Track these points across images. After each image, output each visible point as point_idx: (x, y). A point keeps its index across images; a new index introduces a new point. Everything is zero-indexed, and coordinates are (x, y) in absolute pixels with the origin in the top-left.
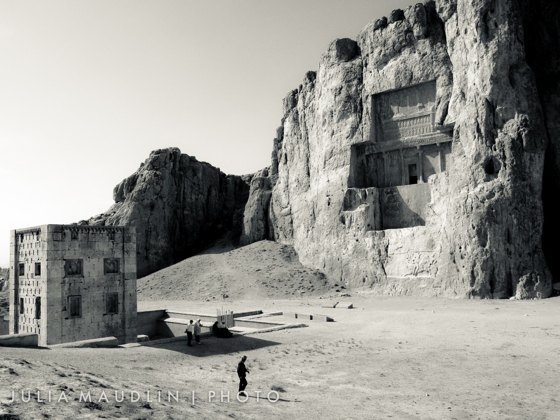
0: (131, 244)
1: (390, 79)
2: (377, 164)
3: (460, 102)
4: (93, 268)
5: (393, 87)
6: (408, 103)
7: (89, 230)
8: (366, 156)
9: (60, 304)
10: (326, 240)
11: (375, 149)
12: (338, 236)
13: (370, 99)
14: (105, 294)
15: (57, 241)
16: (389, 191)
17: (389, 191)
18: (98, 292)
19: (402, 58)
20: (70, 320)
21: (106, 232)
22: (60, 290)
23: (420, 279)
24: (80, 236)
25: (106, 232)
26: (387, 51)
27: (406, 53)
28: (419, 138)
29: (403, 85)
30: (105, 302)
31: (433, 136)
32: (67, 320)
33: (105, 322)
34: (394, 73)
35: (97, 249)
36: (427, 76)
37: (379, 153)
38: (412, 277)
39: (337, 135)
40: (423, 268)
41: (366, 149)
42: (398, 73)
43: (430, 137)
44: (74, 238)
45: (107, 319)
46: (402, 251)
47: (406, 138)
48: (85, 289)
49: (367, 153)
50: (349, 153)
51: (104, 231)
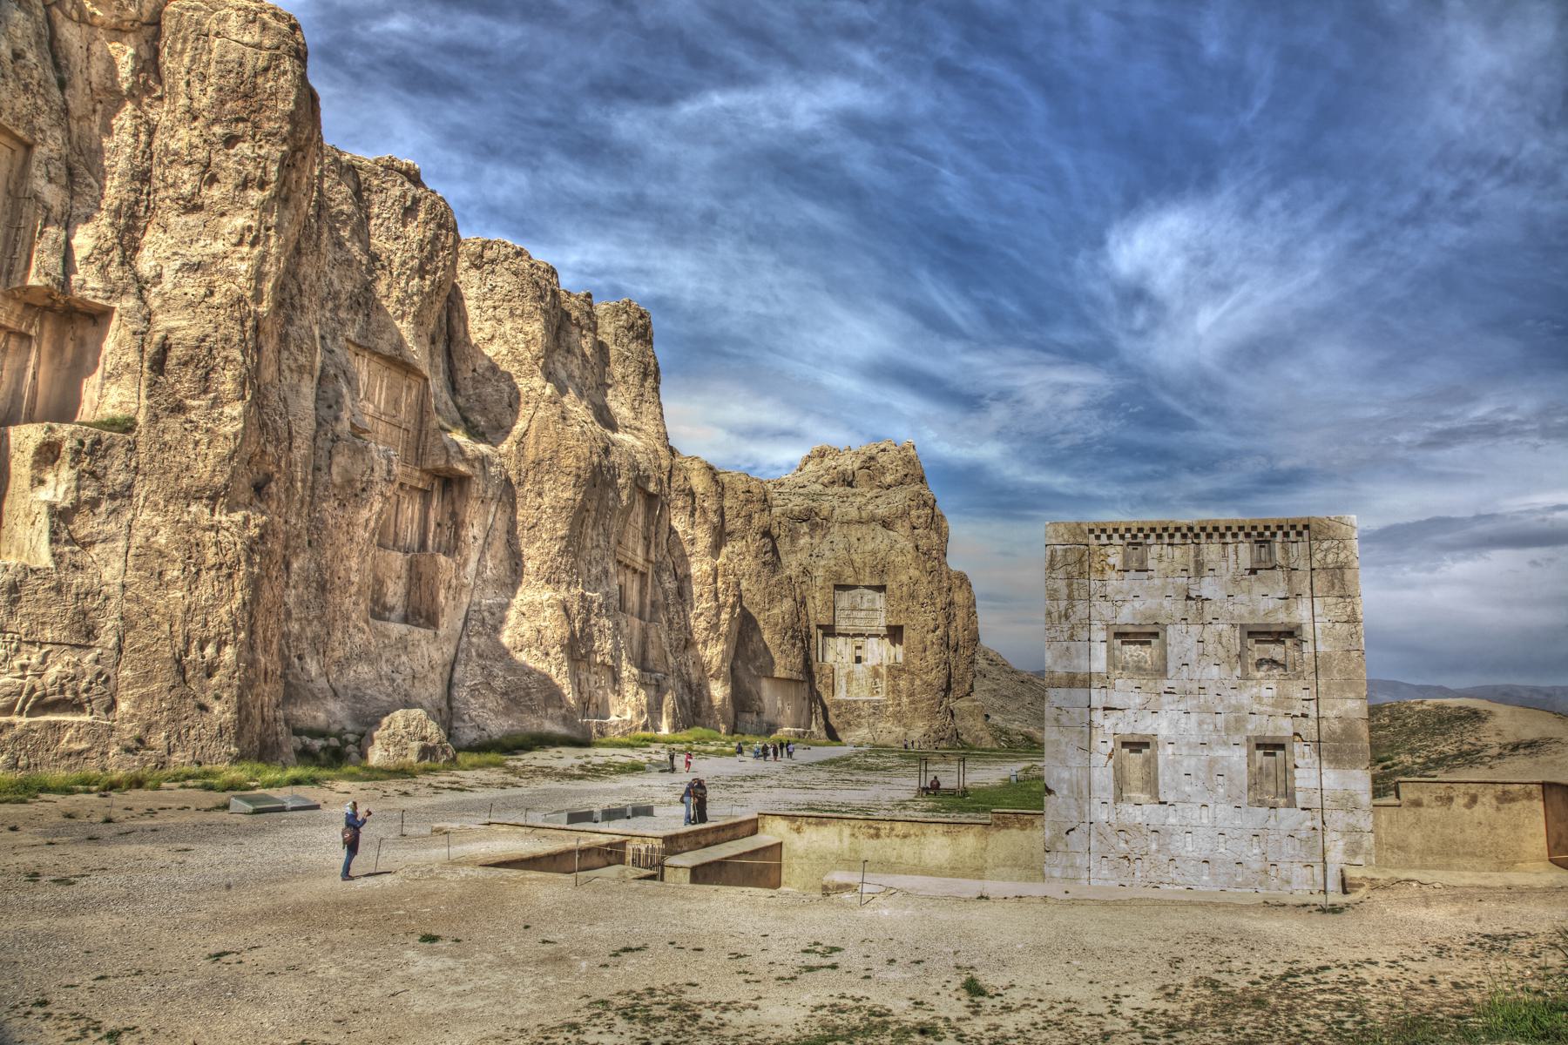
40: (62, 692)
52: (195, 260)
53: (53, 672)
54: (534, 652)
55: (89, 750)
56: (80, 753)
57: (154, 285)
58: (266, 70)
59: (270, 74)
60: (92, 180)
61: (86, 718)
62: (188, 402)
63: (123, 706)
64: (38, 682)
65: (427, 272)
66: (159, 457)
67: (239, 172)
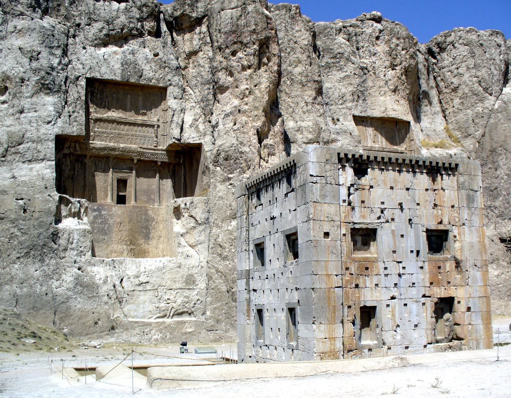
1: (115, 67)
2: (74, 169)
3: (204, 123)
5: (118, 78)
6: (129, 104)
8: (64, 154)
10: (16, 266)
11: (78, 148)
12: (42, 261)
13: (83, 83)
16: (95, 208)
17: (95, 208)
19: (131, 49)
23: (184, 322)
26: (111, 32)
27: (133, 45)
28: (139, 150)
29: (132, 80)
31: (156, 152)
34: (120, 62)
36: (158, 80)
37: (79, 155)
38: (168, 321)
39: (30, 115)
41: (67, 145)
42: (125, 64)
43: (153, 151)
46: (148, 287)
47: (122, 145)
49: (66, 151)
50: (52, 145)
52: (229, 111)
53: (179, 301)
54: (501, 262)
55: (193, 332)
56: (190, 333)
57: (217, 127)
58: (241, 16)
59: (243, 18)
60: (191, 92)
61: (193, 319)
62: (231, 176)
63: (208, 313)
64: (174, 305)
65: (396, 66)
66: (218, 202)
67: (239, 66)
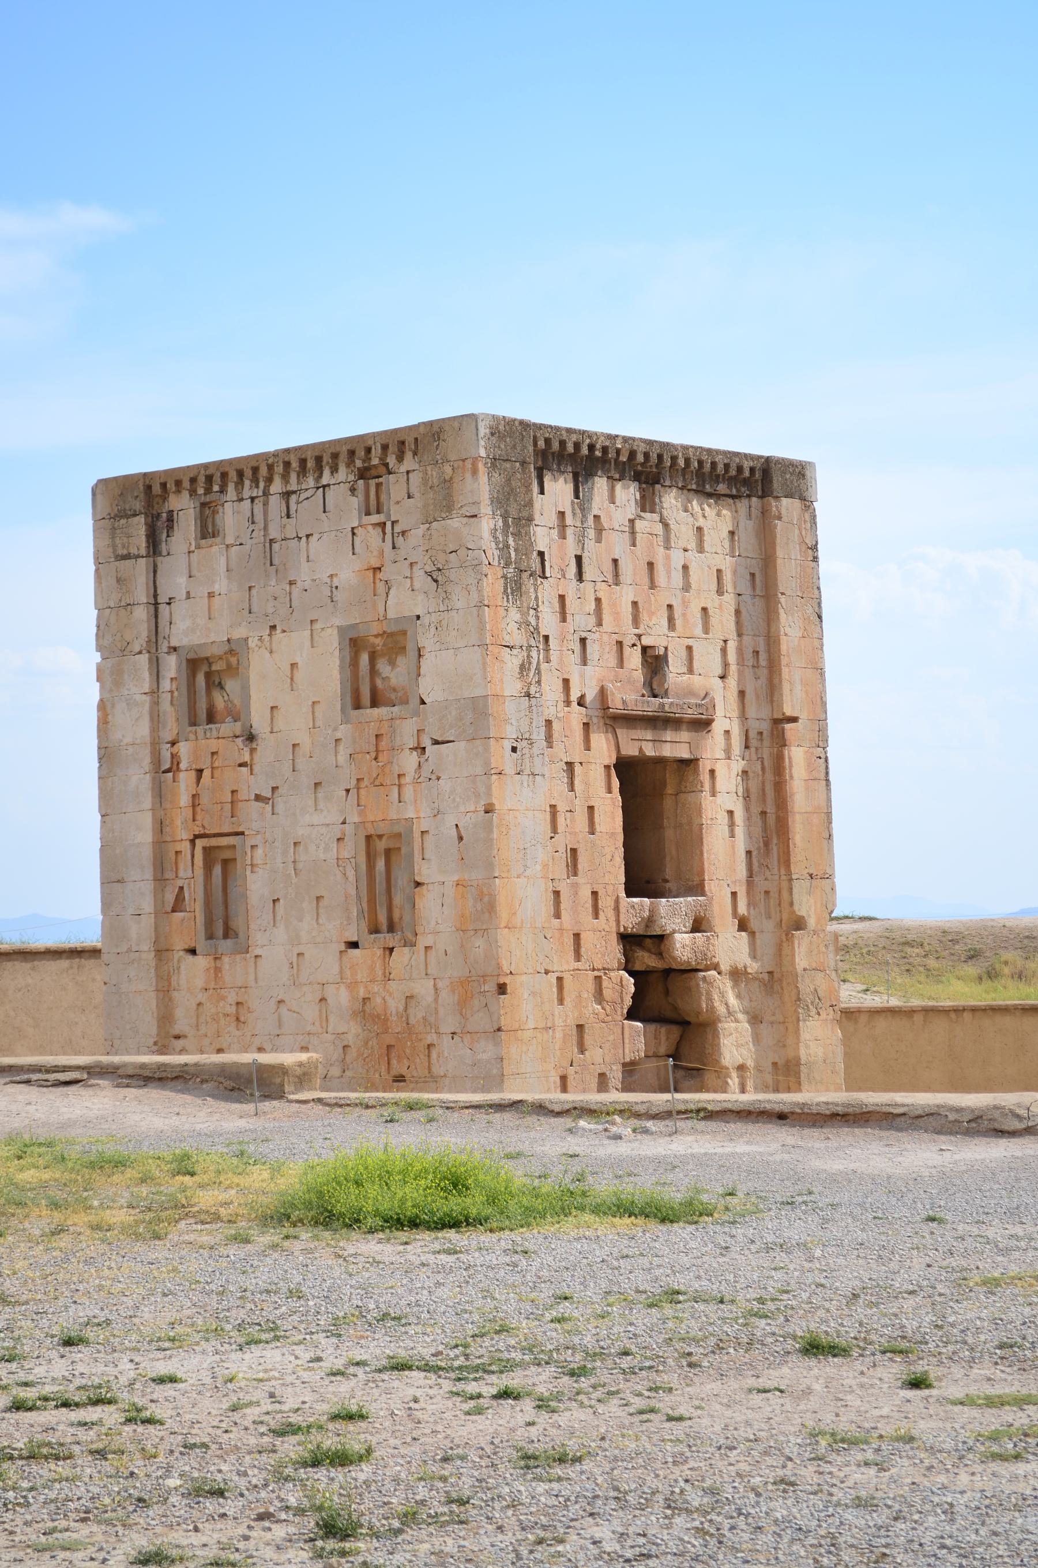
0: (455, 523)
4: (292, 682)
7: (269, 480)
9: (149, 874)
14: (349, 829)
15: (127, 557)
18: (316, 819)
20: (201, 962)
21: (343, 473)
22: (147, 803)
24: (232, 516)
25: (343, 473)
30: (351, 874)
32: (190, 958)
33: (352, 986)
35: (304, 575)
44: (207, 530)
45: (362, 975)
48: (258, 798)
51: (334, 470)
